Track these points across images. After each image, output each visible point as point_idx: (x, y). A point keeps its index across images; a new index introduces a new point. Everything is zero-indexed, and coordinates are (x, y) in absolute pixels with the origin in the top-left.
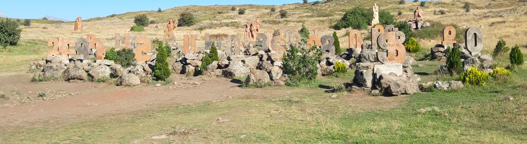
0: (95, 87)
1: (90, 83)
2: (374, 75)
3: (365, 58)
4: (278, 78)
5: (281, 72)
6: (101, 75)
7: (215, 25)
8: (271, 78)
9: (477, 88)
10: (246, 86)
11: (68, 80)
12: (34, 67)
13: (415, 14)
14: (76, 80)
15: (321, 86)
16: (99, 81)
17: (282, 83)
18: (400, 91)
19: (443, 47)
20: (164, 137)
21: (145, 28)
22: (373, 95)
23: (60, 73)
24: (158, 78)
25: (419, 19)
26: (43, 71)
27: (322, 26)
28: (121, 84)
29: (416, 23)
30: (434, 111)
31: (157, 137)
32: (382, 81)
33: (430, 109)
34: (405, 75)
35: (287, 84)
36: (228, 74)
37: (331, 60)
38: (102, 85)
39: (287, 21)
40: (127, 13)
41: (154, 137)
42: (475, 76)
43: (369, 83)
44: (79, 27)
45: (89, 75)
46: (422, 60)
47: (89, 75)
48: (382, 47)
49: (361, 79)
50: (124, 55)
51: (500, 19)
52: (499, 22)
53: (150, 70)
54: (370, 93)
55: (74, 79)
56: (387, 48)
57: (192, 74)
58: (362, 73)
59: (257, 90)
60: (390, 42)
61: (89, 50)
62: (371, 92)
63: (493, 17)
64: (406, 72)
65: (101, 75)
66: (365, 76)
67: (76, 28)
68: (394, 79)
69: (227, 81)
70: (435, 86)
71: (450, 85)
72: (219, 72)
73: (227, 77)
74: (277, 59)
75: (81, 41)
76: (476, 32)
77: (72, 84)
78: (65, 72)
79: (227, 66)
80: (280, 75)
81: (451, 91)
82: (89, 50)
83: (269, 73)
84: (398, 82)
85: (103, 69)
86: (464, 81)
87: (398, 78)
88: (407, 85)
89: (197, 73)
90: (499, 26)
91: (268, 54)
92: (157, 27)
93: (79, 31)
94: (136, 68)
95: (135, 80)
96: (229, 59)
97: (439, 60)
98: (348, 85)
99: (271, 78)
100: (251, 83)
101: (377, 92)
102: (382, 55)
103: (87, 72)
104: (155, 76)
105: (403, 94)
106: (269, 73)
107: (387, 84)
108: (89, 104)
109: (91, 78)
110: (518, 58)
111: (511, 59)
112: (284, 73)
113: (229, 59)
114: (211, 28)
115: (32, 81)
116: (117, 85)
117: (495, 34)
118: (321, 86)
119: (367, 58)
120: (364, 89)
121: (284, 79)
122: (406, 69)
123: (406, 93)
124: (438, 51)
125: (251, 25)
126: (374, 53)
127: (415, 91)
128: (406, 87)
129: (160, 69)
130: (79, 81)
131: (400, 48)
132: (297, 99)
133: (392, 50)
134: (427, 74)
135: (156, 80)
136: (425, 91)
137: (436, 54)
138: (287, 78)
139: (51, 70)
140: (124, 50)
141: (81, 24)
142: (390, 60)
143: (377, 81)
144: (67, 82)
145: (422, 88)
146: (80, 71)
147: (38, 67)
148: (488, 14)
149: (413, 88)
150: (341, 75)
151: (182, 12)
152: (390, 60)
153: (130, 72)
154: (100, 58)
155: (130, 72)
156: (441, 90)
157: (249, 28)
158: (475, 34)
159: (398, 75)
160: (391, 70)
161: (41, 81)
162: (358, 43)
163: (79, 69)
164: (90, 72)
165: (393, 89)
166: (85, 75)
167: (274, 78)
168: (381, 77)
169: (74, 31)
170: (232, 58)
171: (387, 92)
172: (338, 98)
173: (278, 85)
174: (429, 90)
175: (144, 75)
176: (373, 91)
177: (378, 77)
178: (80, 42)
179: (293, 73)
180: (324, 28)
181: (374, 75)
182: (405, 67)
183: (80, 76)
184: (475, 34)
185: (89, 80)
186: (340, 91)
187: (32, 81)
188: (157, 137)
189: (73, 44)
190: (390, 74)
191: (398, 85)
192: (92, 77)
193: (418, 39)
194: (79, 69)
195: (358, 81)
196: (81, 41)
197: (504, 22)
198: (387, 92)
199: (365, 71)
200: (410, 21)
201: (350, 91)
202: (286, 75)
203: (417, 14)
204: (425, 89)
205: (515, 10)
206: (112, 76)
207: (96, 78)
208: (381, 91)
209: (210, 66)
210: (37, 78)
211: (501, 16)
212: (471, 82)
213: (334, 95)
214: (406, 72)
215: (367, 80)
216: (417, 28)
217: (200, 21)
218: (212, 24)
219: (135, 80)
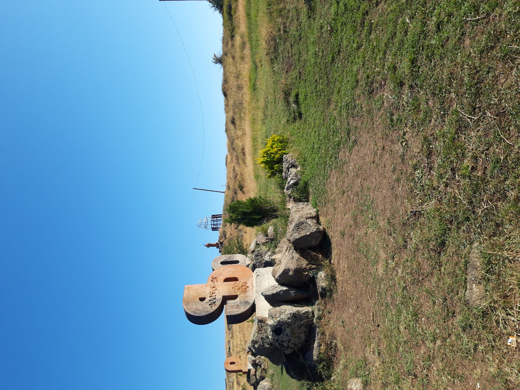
19: (249, 370)
48: (215, 308)
49: (292, 332)
58: (278, 329)
60: (206, 292)
66: (284, 317)
76: (219, 262)
97: (266, 373)
120: (320, 318)
124: (255, 375)
133: (224, 289)
137: (258, 377)
152: (245, 288)
177: (285, 288)
184: (222, 263)
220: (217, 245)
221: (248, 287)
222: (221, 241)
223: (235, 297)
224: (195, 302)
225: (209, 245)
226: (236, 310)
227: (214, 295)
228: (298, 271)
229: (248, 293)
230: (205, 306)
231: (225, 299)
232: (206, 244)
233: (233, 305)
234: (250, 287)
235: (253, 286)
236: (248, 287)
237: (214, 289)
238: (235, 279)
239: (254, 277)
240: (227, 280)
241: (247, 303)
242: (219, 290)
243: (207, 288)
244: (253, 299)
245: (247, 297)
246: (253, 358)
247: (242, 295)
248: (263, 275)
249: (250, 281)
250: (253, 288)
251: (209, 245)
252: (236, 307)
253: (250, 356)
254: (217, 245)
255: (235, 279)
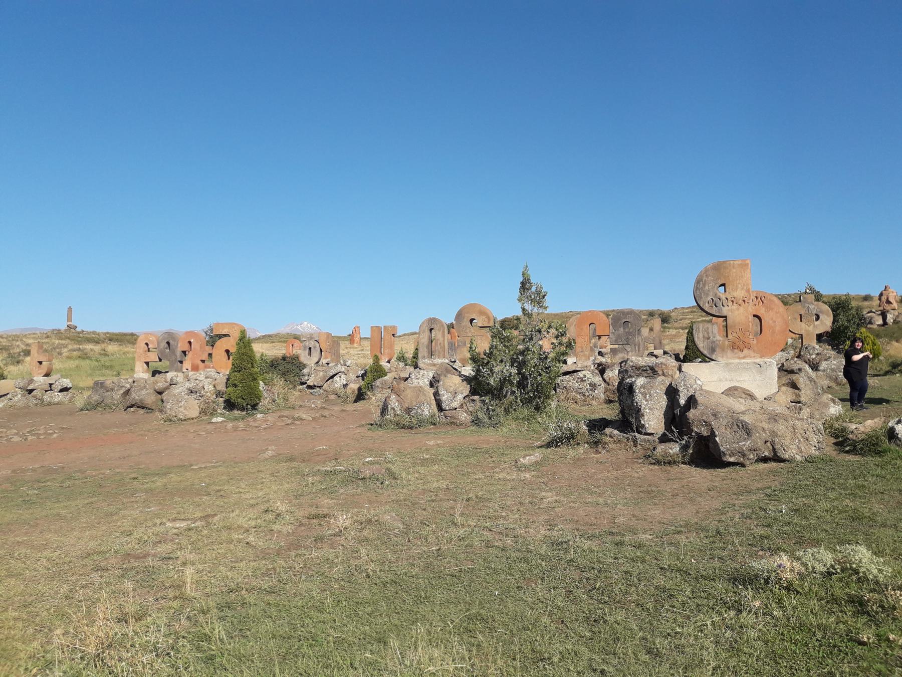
2: (672, 392)
5: (466, 389)
13: (880, 299)
18: (754, 450)
22: (658, 463)
23: (118, 395)
25: (888, 307)
29: (884, 315)
30: (850, 571)
32: (692, 414)
34: (786, 396)
35: (476, 422)
46: (886, 373)
56: (725, 311)
64: (794, 386)
66: (639, 397)
68: (739, 405)
70: (891, 434)
75: (166, 336)
80: (460, 397)
84: (746, 418)
87: (755, 406)
93: (355, 345)
101: (674, 449)
105: (765, 460)
107: (708, 424)
112: (474, 392)
120: (635, 441)
122: (794, 377)
123: (776, 459)
127: (813, 451)
128: (774, 434)
131: (768, 309)
134: (887, 402)
136: (853, 451)
138: (479, 404)
140: (284, 358)
142: (734, 347)
143: (677, 417)
145: (842, 441)
149: (803, 441)
152: (738, 346)
159: (760, 394)
165: (725, 441)
167: (444, 406)
168: (692, 401)
171: (706, 454)
173: (454, 423)
174: (870, 446)
177: (682, 402)
178: (164, 339)
179: (496, 393)
182: (792, 372)
183: (141, 400)
186: (557, 446)
190: (731, 392)
191: (746, 429)
193: (883, 340)
196: (166, 336)
198: (706, 454)
199: (640, 381)
200: (871, 312)
202: (476, 398)
203: (884, 298)
204: (854, 444)
208: (684, 448)
214: (794, 386)
215: (646, 411)
216: (885, 323)
221: (742, 351)
224: (718, 279)
226: (701, 336)
227: (730, 303)
229: (729, 351)
230: (711, 293)
233: (710, 331)
234: (741, 355)
235: (744, 358)
236: (742, 351)
237: (741, 302)
239: (758, 360)
241: (713, 350)
242: (738, 309)
243: (743, 292)
244: (719, 359)
245: (723, 350)
247: (727, 343)
248: (761, 373)
249: (752, 354)
250: (739, 358)
252: (706, 336)
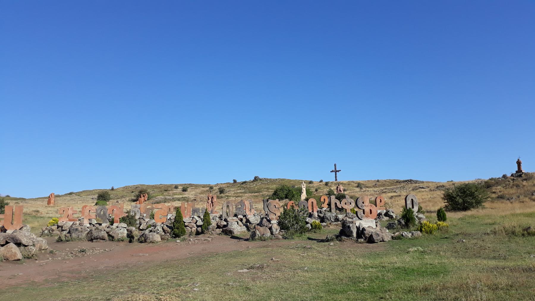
0: (117, 245)
1: (111, 242)
3: (327, 219)
4: (277, 233)
6: (120, 235)
7: (169, 199)
8: (272, 233)
9: (431, 236)
10: (253, 240)
11: (92, 240)
12: (46, 232)
14: (99, 240)
15: (309, 239)
16: (119, 240)
17: (280, 237)
20: (245, 270)
21: (108, 203)
23: (84, 234)
24: (176, 236)
26: (69, 232)
27: (257, 200)
28: (145, 241)
31: (241, 271)
33: (416, 249)
35: (285, 238)
36: (226, 231)
37: (307, 220)
38: (122, 244)
39: (227, 196)
40: (84, 191)
41: (240, 271)
42: (429, 227)
43: (355, 234)
44: (52, 201)
45: (109, 235)
47: (109, 235)
50: (128, 221)
51: (395, 194)
52: (396, 196)
53: (169, 230)
54: (357, 241)
55: (97, 239)
56: (364, 208)
57: (195, 233)
58: (349, 227)
59: (264, 242)
61: (107, 215)
62: (357, 240)
63: (389, 192)
65: (120, 235)
66: (352, 229)
67: (49, 203)
68: (372, 230)
69: (227, 238)
70: (402, 235)
71: (412, 234)
72: (219, 231)
73: (227, 235)
74: (273, 219)
77: (94, 244)
78: (88, 233)
79: (225, 226)
80: (278, 231)
81: (414, 238)
82: (107, 215)
83: (270, 229)
85: (121, 231)
86: (421, 231)
88: (384, 234)
89: (198, 233)
90: (397, 198)
91: (246, 218)
92: (117, 202)
93: (51, 205)
94: (156, 228)
95: (157, 238)
96: (226, 220)
98: (337, 237)
99: (272, 233)
100: (257, 237)
101: (362, 240)
102: (360, 212)
103: (107, 233)
104: (174, 234)
105: (381, 241)
106: (270, 229)
108: (141, 254)
109: (111, 238)
110: (443, 216)
111: (438, 217)
112: (281, 229)
113: (226, 220)
114: (165, 202)
115: (58, 241)
116: (141, 242)
117: (398, 204)
118: (309, 239)
119: (329, 218)
121: (281, 233)
125: (212, 198)
126: (334, 215)
129: (178, 229)
130: (101, 241)
132: (309, 246)
133: (367, 210)
135: (175, 238)
136: (395, 239)
139: (77, 232)
141: (53, 199)
143: (361, 233)
144: (90, 242)
145: (392, 237)
146: (102, 232)
147: (51, 232)
148: (384, 191)
150: (318, 231)
151: (139, 189)
153: (151, 231)
154: (117, 222)
155: (151, 231)
156: (407, 237)
157: (210, 200)
158: (412, 200)
160: (368, 224)
161: (68, 241)
162: (314, 209)
163: (101, 230)
164: (110, 233)
165: (375, 237)
166: (106, 236)
169: (47, 205)
170: (228, 220)
171: (370, 240)
172: (335, 245)
173: (278, 239)
175: (163, 233)
176: (359, 240)
180: (259, 202)
181: (358, 228)
183: (103, 236)
184: (412, 200)
185: (110, 240)
187: (58, 241)
188: (241, 271)
189: (93, 210)
190: (369, 227)
191: (378, 235)
192: (113, 237)
194: (101, 230)
195: (345, 232)
197: (400, 196)
199: (351, 225)
201: (340, 240)
203: (339, 189)
205: (404, 187)
206: (128, 236)
207: (116, 238)
208: (365, 239)
209: (211, 227)
210: (63, 239)
211: (395, 192)
212: (427, 233)
213: (332, 244)
217: (155, 197)
218: (166, 199)
219: (157, 238)
220: (519, 170)
222: (523, 175)
223: (364, 213)
225: (519, 163)
228: (364, 234)
231: (364, 210)
232: (521, 160)
238: (371, 213)
240: (371, 210)
246: (383, 214)
251: (519, 163)
253: (385, 211)
254: (519, 170)
255: (371, 213)
